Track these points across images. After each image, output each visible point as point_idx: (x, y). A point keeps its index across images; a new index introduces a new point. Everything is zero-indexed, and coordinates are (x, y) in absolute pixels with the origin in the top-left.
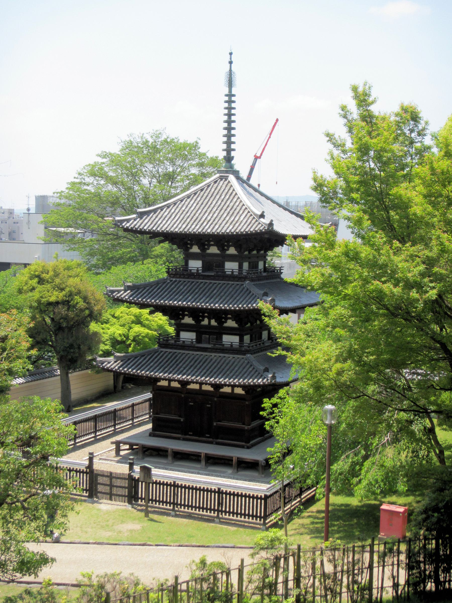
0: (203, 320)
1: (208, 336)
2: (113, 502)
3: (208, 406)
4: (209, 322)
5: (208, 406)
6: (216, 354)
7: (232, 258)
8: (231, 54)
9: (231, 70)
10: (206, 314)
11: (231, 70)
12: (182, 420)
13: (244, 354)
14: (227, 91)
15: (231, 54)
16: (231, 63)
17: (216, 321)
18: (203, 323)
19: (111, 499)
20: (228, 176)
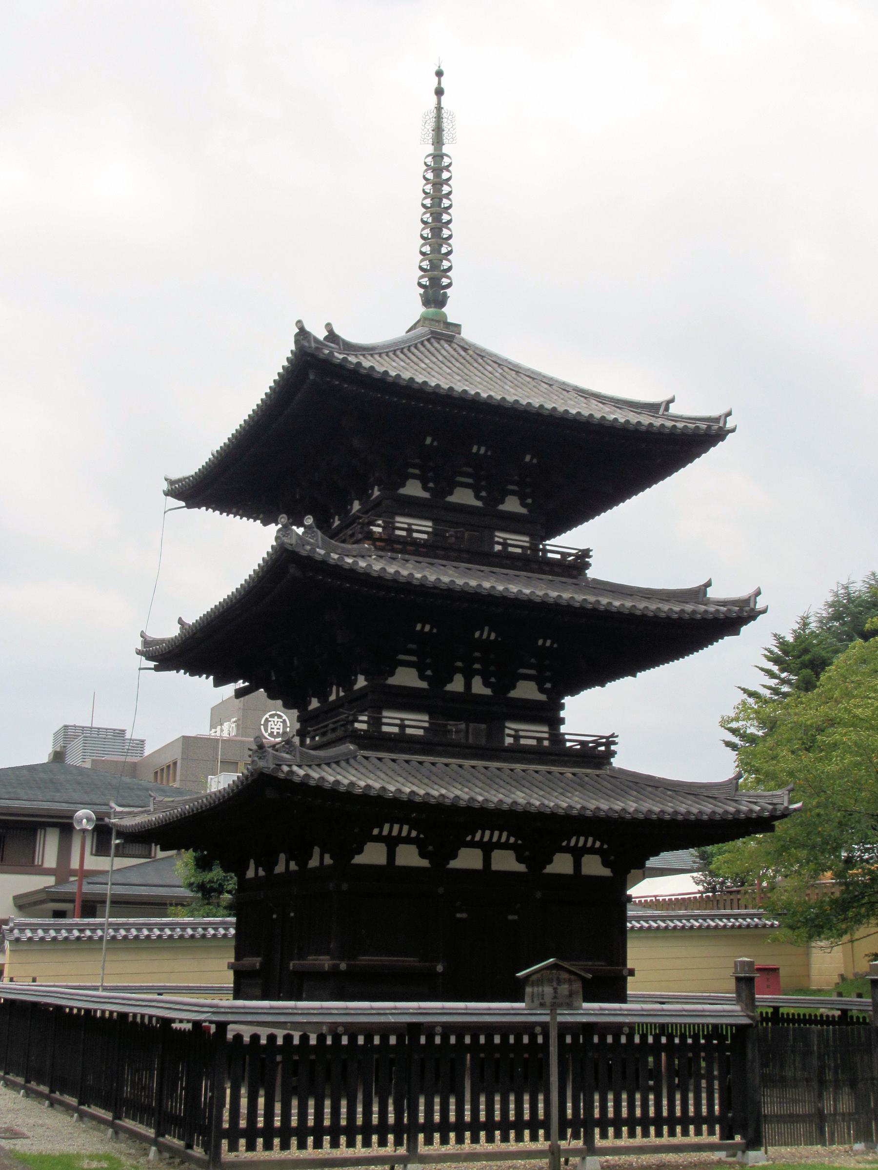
0: (451, 680)
1: (463, 726)
3: (510, 917)
4: (468, 685)
5: (510, 917)
6: (524, 767)
7: (512, 523)
8: (439, 74)
9: (439, 109)
10: (459, 664)
11: (439, 109)
12: (440, 968)
14: (430, 149)
15: (439, 74)
16: (439, 92)
17: (486, 684)
18: (449, 687)
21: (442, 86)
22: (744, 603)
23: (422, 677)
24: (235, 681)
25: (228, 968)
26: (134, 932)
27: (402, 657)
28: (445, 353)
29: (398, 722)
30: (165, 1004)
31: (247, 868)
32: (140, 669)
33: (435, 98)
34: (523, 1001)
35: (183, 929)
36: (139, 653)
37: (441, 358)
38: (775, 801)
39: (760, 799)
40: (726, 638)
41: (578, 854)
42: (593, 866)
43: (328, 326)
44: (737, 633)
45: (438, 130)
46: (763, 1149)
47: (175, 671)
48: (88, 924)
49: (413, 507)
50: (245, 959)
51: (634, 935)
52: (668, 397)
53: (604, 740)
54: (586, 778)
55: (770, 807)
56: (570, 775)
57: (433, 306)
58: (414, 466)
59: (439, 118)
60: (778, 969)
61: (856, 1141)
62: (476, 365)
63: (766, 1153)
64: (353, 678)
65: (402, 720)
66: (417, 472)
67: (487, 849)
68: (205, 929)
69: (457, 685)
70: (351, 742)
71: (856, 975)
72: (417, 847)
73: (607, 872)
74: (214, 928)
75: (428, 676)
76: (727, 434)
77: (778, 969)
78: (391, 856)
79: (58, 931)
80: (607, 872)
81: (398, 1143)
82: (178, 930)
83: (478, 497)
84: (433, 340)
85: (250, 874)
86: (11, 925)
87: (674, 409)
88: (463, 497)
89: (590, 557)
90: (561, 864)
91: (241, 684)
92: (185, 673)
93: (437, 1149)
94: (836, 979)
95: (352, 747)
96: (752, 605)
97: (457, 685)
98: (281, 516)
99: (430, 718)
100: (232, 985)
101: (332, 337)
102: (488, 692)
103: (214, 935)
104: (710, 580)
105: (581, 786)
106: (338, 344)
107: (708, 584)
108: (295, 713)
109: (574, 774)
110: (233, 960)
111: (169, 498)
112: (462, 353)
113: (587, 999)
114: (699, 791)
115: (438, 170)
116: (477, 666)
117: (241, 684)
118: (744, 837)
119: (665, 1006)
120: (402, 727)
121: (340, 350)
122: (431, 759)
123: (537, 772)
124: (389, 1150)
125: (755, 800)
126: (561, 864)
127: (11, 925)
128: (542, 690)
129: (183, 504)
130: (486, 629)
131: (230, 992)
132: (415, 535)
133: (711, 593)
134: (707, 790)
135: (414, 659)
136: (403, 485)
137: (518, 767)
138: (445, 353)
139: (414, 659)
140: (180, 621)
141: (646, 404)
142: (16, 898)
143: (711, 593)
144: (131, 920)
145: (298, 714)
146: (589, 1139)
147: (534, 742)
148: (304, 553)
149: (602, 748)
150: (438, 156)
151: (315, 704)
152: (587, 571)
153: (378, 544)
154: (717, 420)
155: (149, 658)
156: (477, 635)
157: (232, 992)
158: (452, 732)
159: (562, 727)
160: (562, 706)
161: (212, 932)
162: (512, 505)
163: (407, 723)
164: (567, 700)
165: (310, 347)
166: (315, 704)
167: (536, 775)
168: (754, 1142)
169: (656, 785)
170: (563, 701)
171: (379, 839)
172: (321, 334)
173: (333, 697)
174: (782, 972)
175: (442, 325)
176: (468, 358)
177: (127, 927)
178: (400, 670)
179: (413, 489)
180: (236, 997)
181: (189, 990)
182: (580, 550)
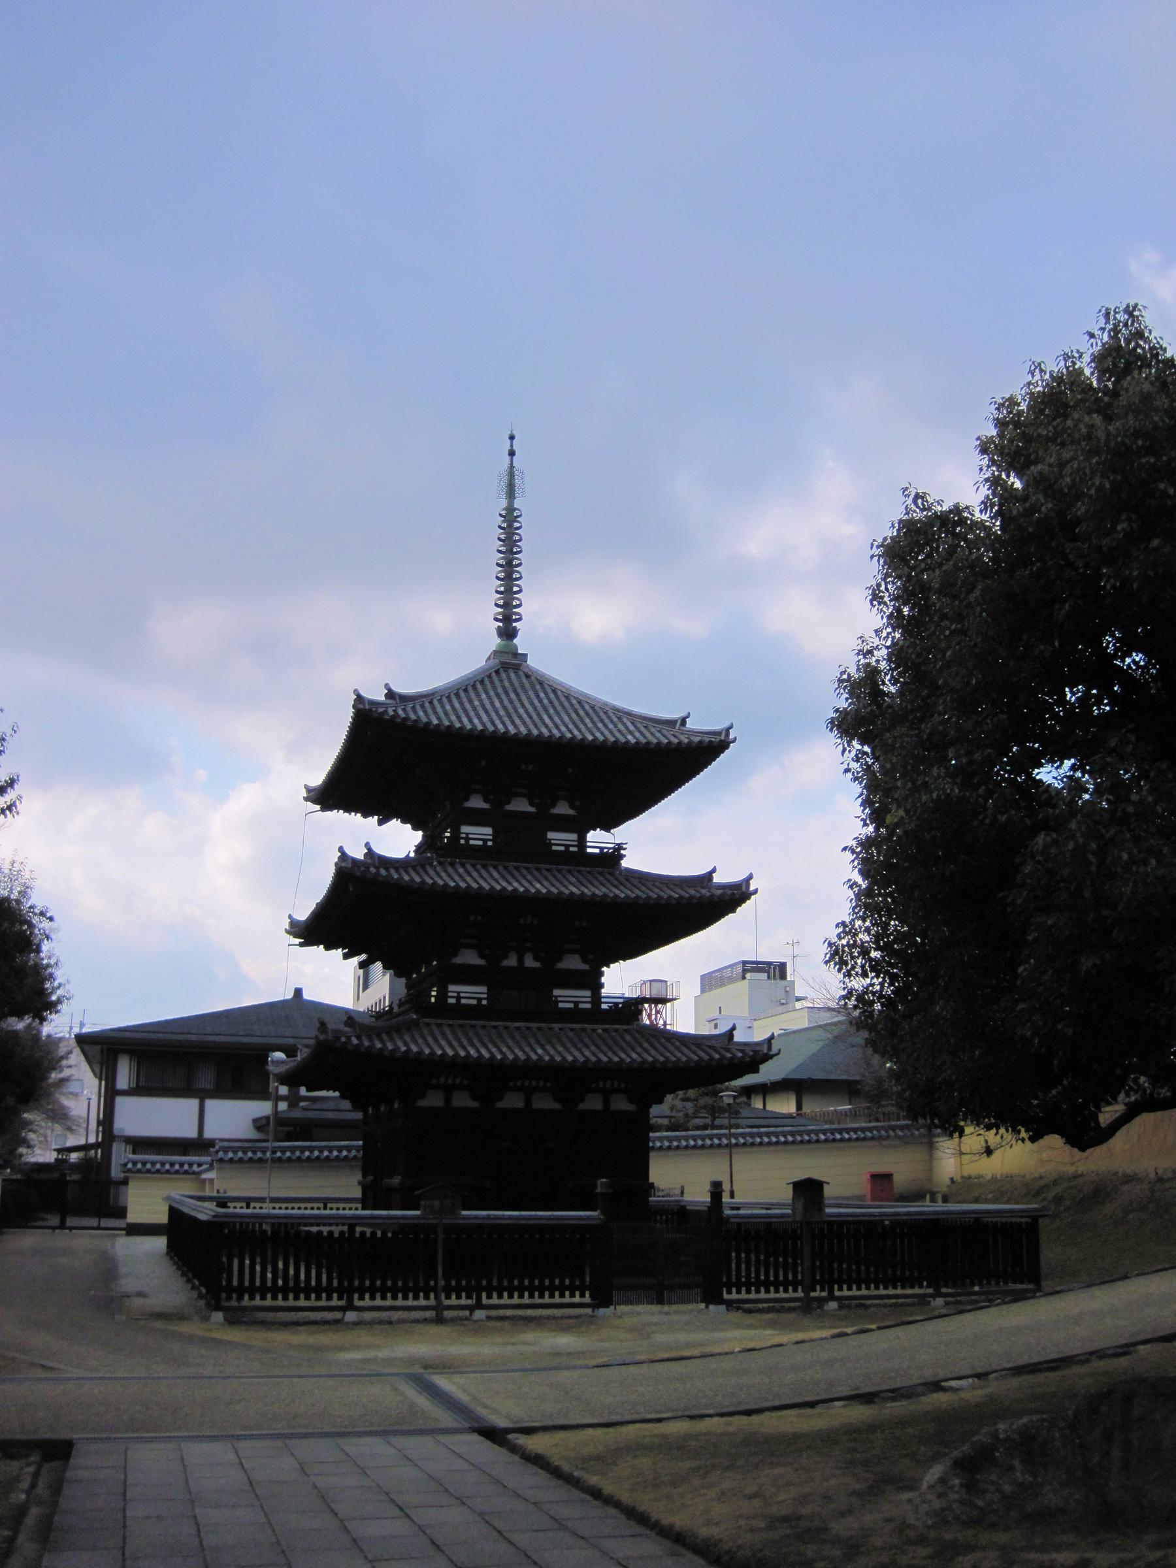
0: (506, 958)
2: (666, 1308)
4: (521, 960)
6: (561, 1025)
7: (563, 824)
8: (512, 438)
9: (512, 467)
11: (512, 467)
13: (628, 1023)
14: (504, 503)
15: (512, 438)
16: (512, 453)
17: (536, 959)
18: (505, 963)
19: (661, 1301)
20: (520, 665)
21: (514, 448)
24: (360, 954)
26: (335, 1153)
28: (507, 684)
29: (455, 995)
32: (289, 945)
33: (508, 458)
34: (419, 1210)
36: (288, 932)
37: (500, 690)
38: (758, 1048)
41: (606, 1095)
42: (621, 1104)
43: (387, 686)
44: (733, 910)
46: (612, 1307)
48: (280, 1147)
49: (477, 818)
51: (740, 1150)
52: (683, 714)
54: (614, 1034)
55: (751, 1053)
56: (600, 1031)
57: (505, 638)
60: (892, 1175)
61: (702, 1302)
62: (531, 693)
63: (615, 1309)
65: (459, 993)
67: (528, 1093)
69: (511, 961)
70: (416, 1013)
71: (962, 1177)
77: (892, 1175)
78: (448, 1099)
79: (254, 1153)
81: (340, 1298)
83: (531, 804)
84: (501, 671)
86: (217, 1147)
87: (689, 724)
88: (521, 805)
89: (625, 849)
90: (593, 1103)
91: (363, 957)
93: (367, 1302)
94: (949, 1183)
95: (415, 1017)
96: (744, 888)
97: (511, 961)
99: (488, 990)
101: (391, 694)
102: (537, 965)
105: (604, 1041)
106: (395, 699)
107: (714, 870)
108: (403, 980)
109: (604, 1030)
110: (359, 1177)
112: (525, 680)
113: (464, 1210)
115: (510, 518)
116: (529, 944)
117: (363, 957)
119: (769, 1212)
120: (458, 998)
121: (397, 703)
122: (482, 1023)
123: (572, 1030)
124: (335, 1302)
126: (593, 1103)
127: (217, 1147)
128: (585, 961)
129: (318, 807)
130: (529, 917)
132: (472, 842)
133: (717, 879)
136: (467, 799)
137: (556, 1026)
138: (507, 684)
141: (667, 720)
142: (255, 1121)
143: (717, 879)
144: (314, 1144)
146: (479, 1299)
147: (571, 1005)
148: (358, 873)
150: (510, 509)
152: (622, 862)
153: (440, 852)
154: (718, 733)
156: (522, 921)
159: (603, 991)
160: (602, 974)
162: (562, 809)
163: (462, 995)
167: (571, 1034)
168: (606, 1303)
172: (380, 696)
174: (897, 1178)
175: (510, 656)
176: (527, 686)
177: (311, 1149)
179: (476, 802)
180: (364, 1208)
182: (617, 844)
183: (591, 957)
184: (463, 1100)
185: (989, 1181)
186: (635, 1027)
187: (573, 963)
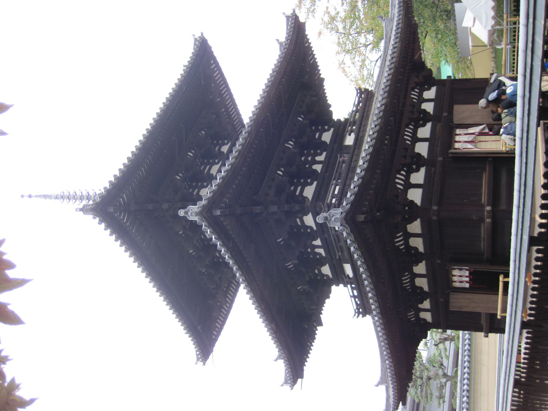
0: (316, 170)
9: (37, 196)
11: (37, 196)
15: (22, 196)
16: (30, 196)
17: (320, 154)
22: (288, 17)
23: (311, 184)
25: (487, 336)
27: (297, 193)
30: (513, 310)
31: (425, 320)
32: (301, 389)
33: (33, 198)
35: (463, 403)
39: (394, 3)
40: (306, 33)
45: (45, 196)
47: (304, 367)
50: (482, 323)
53: (358, 95)
58: (193, 191)
59: (40, 196)
64: (309, 230)
66: (196, 191)
68: (464, 391)
69: (318, 168)
72: (412, 173)
73: (434, 89)
74: (464, 386)
75: (311, 181)
76: (204, 37)
80: (434, 89)
82: (463, 405)
85: (427, 316)
92: (307, 362)
98: (179, 214)
100: (499, 334)
103: (468, 385)
104: (276, 39)
107: (278, 40)
108: (334, 288)
110: (482, 334)
111: (206, 363)
114: (388, 37)
115: (63, 197)
118: (418, 34)
125: (394, 6)
129: (211, 354)
130: (286, 145)
131: (502, 336)
133: (283, 39)
134: (388, 33)
135: (299, 188)
139: (299, 188)
140: (276, 360)
145: (334, 285)
149: (363, 95)
151: (326, 270)
154: (196, 40)
155: (294, 382)
157: (502, 334)
158: (343, 159)
160: (339, 121)
161: (466, 387)
164: (335, 117)
165: (92, 204)
166: (326, 270)
169: (384, 60)
170: (336, 120)
171: (405, 191)
173: (321, 251)
178: (305, 194)
181: (500, 368)
183: (326, 127)
184: (418, 177)
185: (495, 63)
186: (376, 90)
187: (327, 137)
